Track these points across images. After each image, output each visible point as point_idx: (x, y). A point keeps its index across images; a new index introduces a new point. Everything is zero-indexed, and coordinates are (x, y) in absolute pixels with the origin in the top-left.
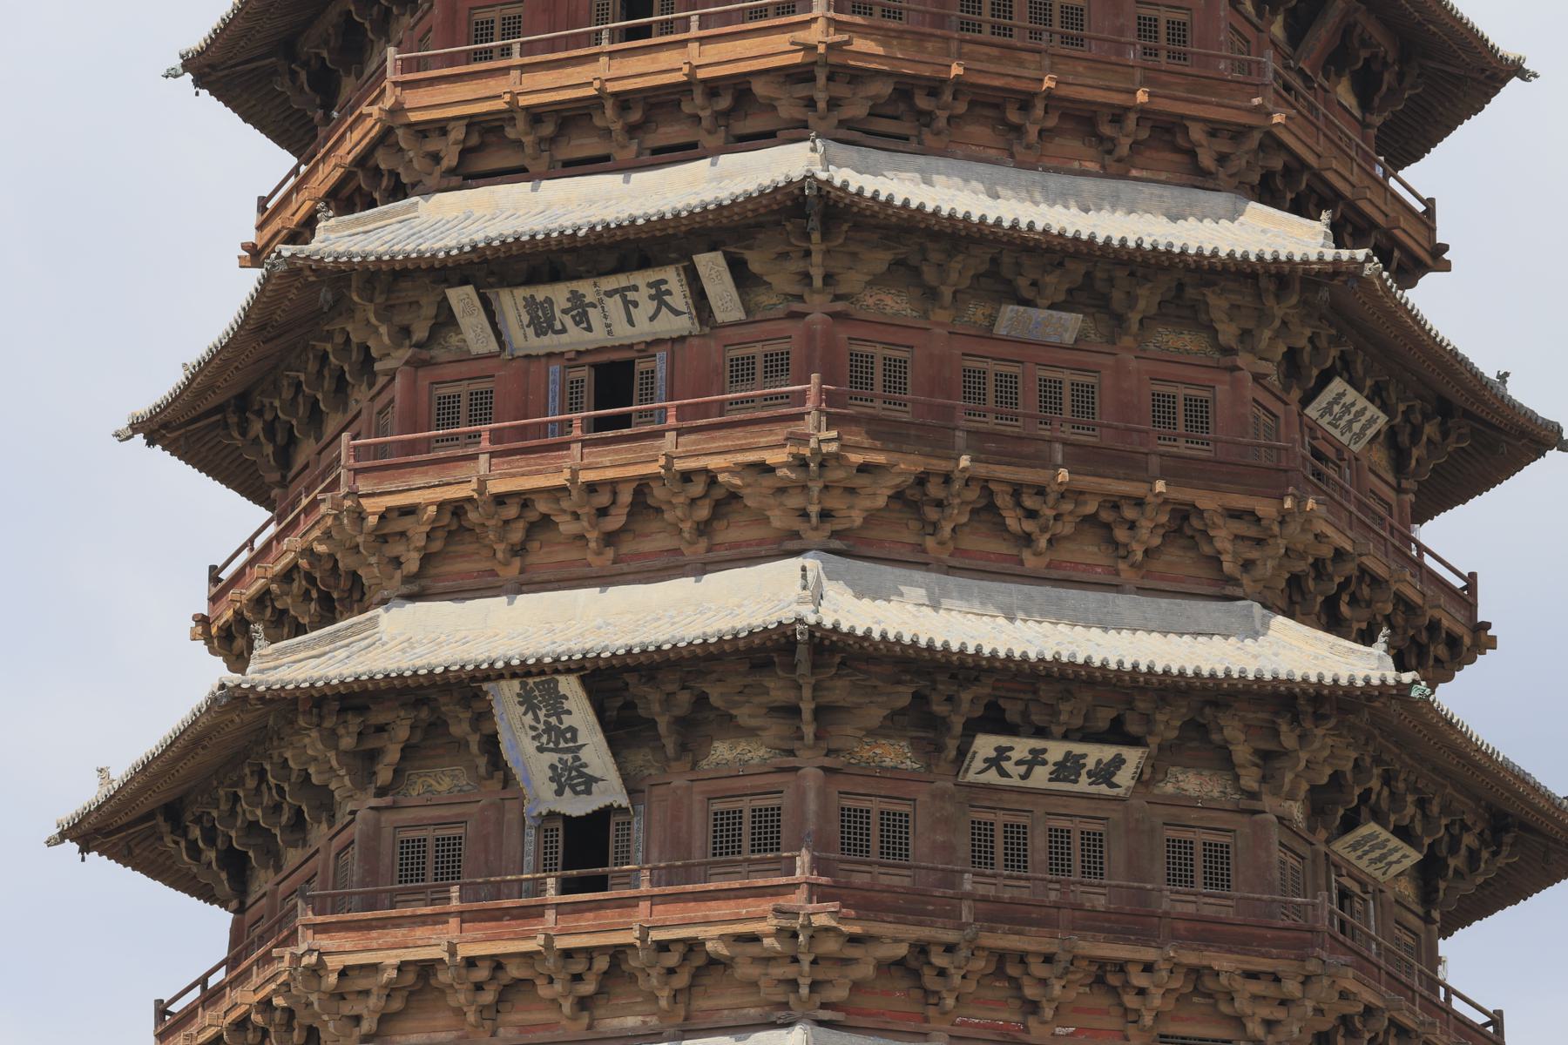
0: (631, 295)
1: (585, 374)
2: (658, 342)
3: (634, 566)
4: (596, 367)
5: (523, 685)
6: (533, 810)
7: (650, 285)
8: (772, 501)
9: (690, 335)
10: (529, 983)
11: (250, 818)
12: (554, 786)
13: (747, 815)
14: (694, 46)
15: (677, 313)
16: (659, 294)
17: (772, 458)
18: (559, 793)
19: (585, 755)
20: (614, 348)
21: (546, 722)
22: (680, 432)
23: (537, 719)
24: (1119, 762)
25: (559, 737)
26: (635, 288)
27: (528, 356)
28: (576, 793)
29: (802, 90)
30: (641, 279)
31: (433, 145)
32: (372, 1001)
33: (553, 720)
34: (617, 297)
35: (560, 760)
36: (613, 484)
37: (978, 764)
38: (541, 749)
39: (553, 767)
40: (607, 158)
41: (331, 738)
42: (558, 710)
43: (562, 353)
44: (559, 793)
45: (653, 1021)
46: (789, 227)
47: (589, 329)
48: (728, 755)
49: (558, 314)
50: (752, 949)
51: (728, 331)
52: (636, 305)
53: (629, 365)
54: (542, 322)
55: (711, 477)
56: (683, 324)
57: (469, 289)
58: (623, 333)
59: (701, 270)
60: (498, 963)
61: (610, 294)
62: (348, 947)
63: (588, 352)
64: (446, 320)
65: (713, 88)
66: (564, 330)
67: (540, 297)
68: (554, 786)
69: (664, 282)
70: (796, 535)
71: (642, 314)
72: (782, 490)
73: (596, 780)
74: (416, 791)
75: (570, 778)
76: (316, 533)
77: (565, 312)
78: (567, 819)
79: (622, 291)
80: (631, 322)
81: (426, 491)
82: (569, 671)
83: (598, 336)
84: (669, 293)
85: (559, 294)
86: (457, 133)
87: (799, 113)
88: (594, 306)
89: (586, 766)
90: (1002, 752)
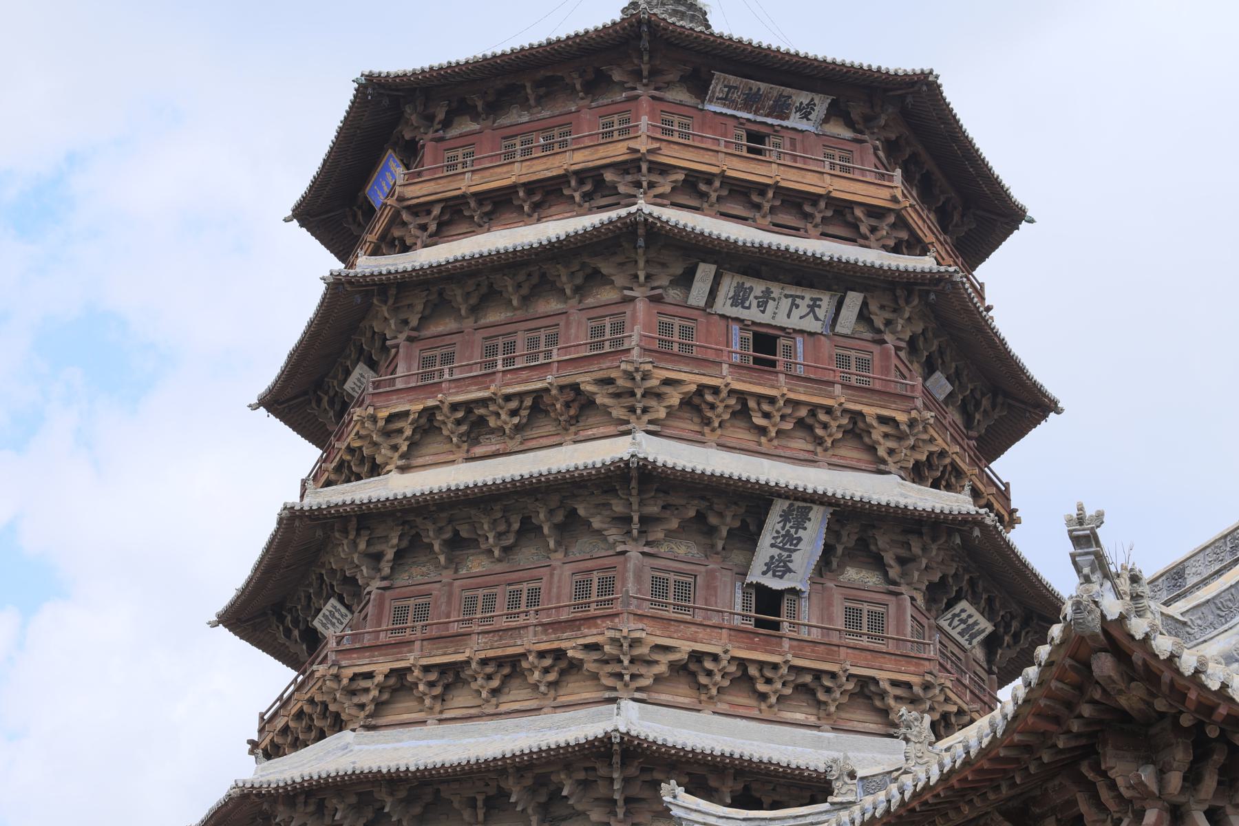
0: (798, 301)
1: (750, 335)
2: (801, 332)
3: (788, 453)
4: (756, 334)
5: (791, 505)
6: (749, 580)
7: (812, 299)
8: (881, 440)
9: (821, 334)
10: (751, 680)
11: (464, 534)
12: (765, 568)
13: (865, 614)
14: (827, 177)
15: (817, 319)
16: (812, 308)
17: (901, 417)
18: (764, 573)
19: (795, 556)
20: (775, 327)
21: (788, 531)
22: (844, 386)
23: (783, 528)
24: (983, 631)
25: (790, 542)
26: (803, 298)
27: (723, 316)
28: (774, 575)
29: (873, 222)
30: (809, 294)
31: (654, 178)
32: (657, 669)
33: (793, 531)
34: (790, 300)
35: (780, 555)
36: (796, 404)
37: (949, 616)
38: (772, 546)
39: (772, 557)
40: (745, 219)
41: (642, 503)
42: (800, 526)
43: (742, 321)
44: (764, 573)
45: (812, 719)
46: (899, 292)
47: (763, 312)
48: (855, 577)
49: (751, 297)
50: (898, 692)
51: (837, 338)
52: (797, 307)
53: (776, 338)
54: (739, 300)
55: (856, 416)
56: (814, 326)
57: (713, 267)
58: (782, 320)
59: (847, 301)
60: (742, 663)
61: (786, 296)
62: (658, 633)
63: (760, 325)
64: (686, 280)
65: (831, 201)
66: (748, 308)
67: (747, 285)
68: (765, 568)
69: (821, 300)
70: (884, 462)
71: (796, 313)
72: (886, 436)
73: (790, 571)
74: (663, 550)
75: (777, 566)
76: (588, 379)
77: (756, 298)
78: (760, 589)
79: (794, 297)
80: (789, 316)
81: (692, 379)
82: (830, 504)
83: (765, 318)
84: (819, 306)
85: (758, 287)
86: (680, 177)
87: (868, 234)
88: (774, 300)
89: (791, 561)
90: (963, 611)
